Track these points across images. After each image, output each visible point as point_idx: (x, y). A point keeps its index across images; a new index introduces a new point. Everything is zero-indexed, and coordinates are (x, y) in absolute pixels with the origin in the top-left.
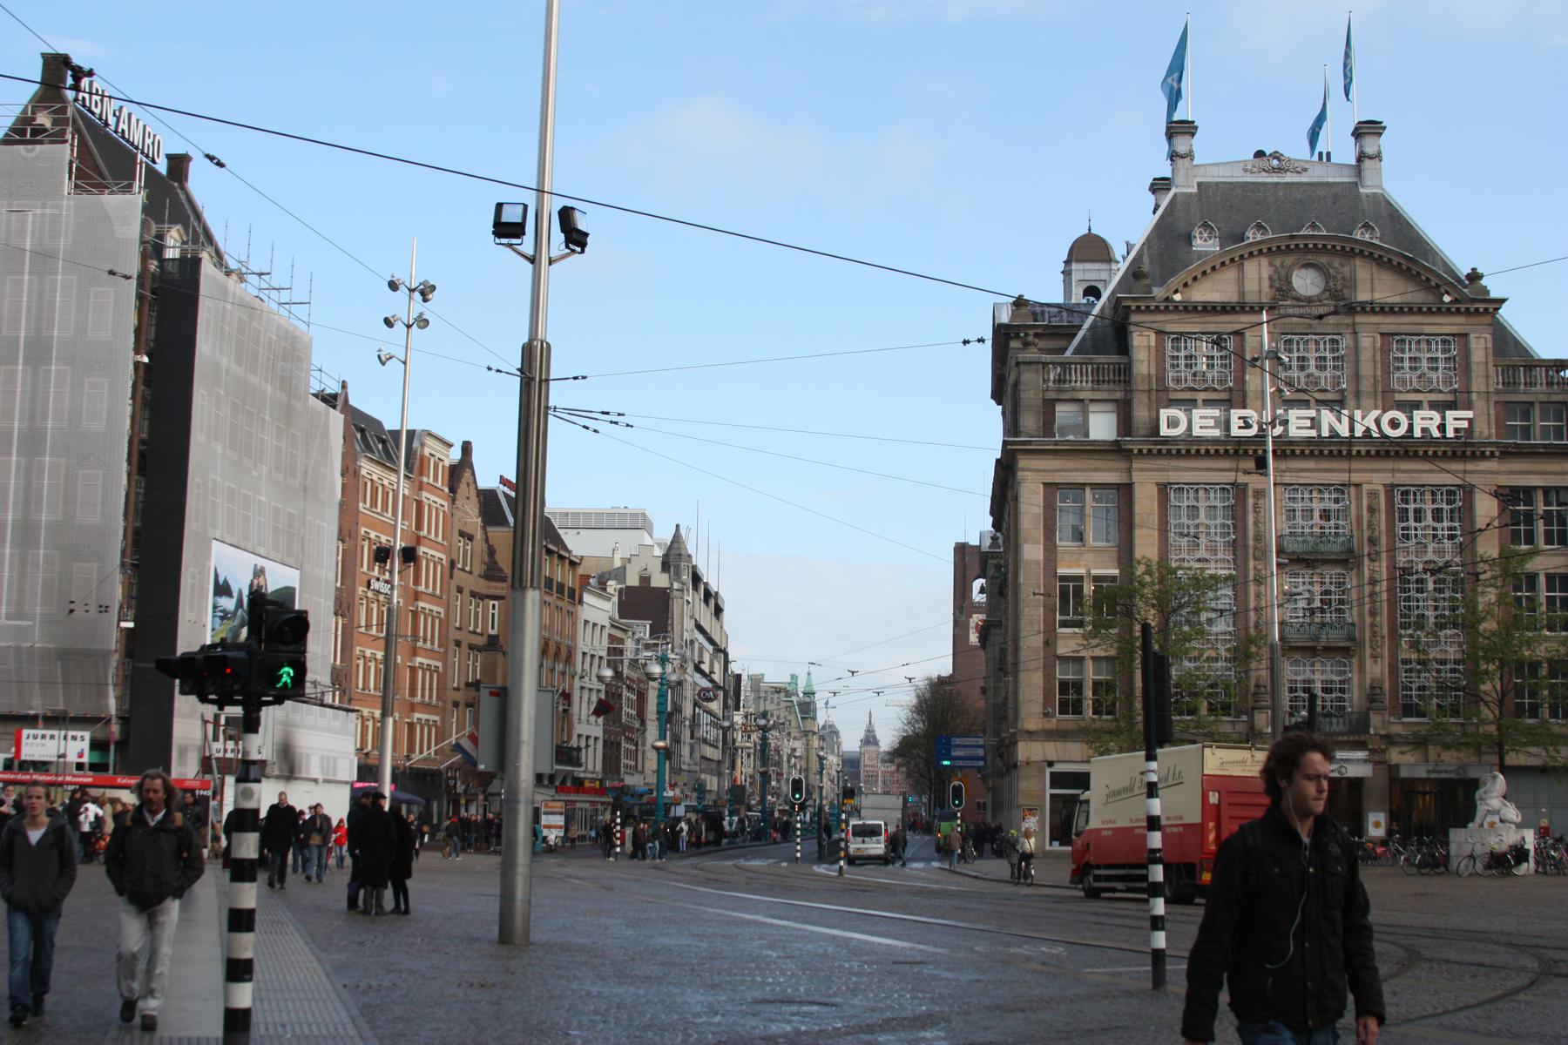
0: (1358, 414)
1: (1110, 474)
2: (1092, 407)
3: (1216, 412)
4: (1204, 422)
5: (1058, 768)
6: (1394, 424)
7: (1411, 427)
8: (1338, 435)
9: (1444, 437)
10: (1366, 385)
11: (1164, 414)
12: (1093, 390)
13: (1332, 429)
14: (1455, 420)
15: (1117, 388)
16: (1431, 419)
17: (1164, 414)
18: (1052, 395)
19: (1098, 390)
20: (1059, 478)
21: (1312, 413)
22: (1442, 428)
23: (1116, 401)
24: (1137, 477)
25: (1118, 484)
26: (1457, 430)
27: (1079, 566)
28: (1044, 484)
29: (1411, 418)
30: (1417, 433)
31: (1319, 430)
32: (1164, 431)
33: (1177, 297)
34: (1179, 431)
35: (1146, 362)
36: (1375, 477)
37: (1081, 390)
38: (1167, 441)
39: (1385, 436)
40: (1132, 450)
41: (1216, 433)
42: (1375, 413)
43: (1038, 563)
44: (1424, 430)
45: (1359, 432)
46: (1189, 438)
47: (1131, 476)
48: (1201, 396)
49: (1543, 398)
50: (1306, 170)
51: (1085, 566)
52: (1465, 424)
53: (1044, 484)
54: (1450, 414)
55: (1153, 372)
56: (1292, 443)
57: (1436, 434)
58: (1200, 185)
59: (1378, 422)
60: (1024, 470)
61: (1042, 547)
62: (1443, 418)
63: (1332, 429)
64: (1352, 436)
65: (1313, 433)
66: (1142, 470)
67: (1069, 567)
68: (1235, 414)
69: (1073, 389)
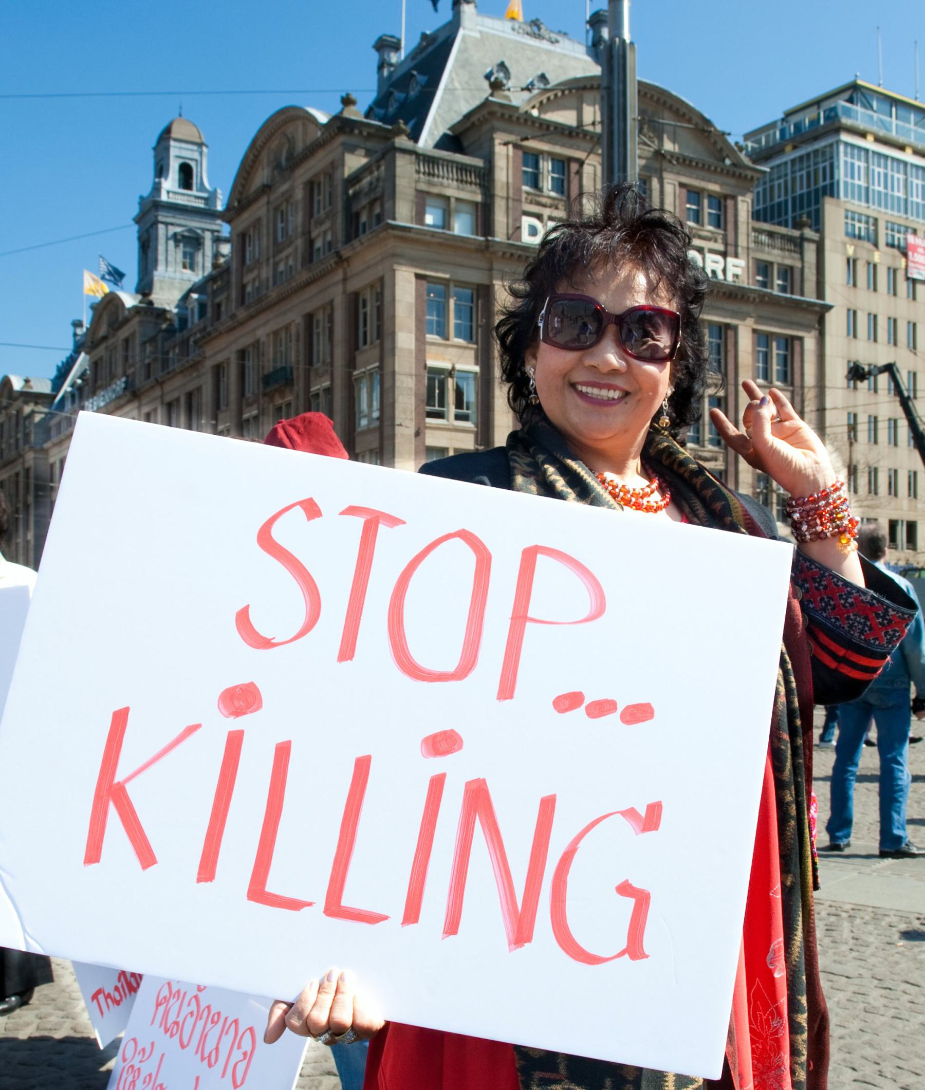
11: (526, 221)
12: (458, 188)
16: (716, 262)
17: (526, 221)
18: (423, 187)
19: (463, 190)
22: (724, 271)
27: (444, 359)
33: (535, 113)
35: (505, 171)
37: (448, 187)
43: (410, 351)
50: (557, 41)
51: (450, 360)
52: (739, 271)
54: (731, 260)
55: (511, 180)
57: (720, 276)
58: (481, 32)
61: (413, 336)
67: (436, 359)
69: (442, 185)
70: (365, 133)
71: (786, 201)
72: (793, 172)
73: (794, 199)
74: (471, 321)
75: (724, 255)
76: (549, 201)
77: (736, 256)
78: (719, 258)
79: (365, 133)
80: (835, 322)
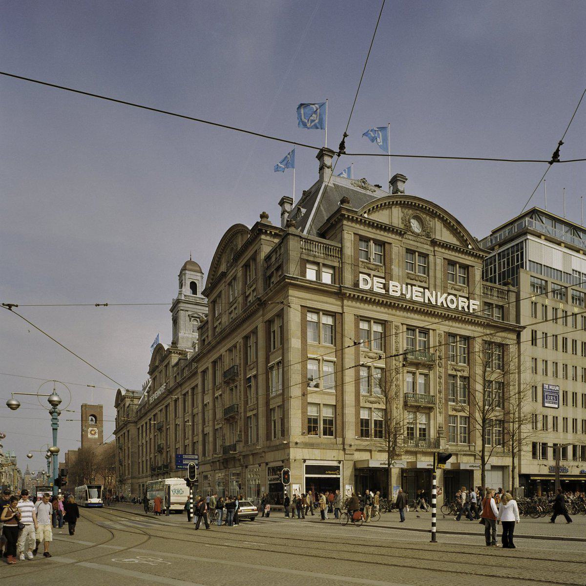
0: (439, 294)
1: (332, 305)
2: (324, 269)
3: (383, 281)
4: (377, 285)
5: (309, 463)
6: (452, 301)
7: (457, 306)
8: (431, 303)
9: (469, 312)
10: (438, 282)
11: (362, 276)
13: (429, 300)
14: (475, 305)
15: (335, 260)
17: (362, 276)
20: (309, 304)
21: (422, 290)
22: (468, 307)
23: (333, 268)
24: (346, 309)
25: (336, 313)
26: (474, 309)
28: (301, 306)
29: (458, 300)
30: (460, 309)
31: (424, 300)
32: (362, 286)
34: (367, 287)
36: (444, 327)
38: (362, 291)
39: (448, 307)
40: (346, 293)
41: (383, 291)
42: (445, 295)
44: (463, 308)
45: (439, 304)
46: (371, 291)
47: (343, 309)
48: (372, 273)
49: (496, 303)
52: (475, 307)
53: (301, 306)
56: (414, 302)
59: (446, 300)
60: (291, 296)
62: (469, 303)
63: (429, 300)
64: (436, 305)
65: (421, 300)
66: (349, 306)
68: (391, 283)
70: (273, 233)
71: (495, 276)
72: (499, 260)
73: (499, 274)
74: (332, 334)
75: (468, 299)
76: (374, 267)
77: (474, 299)
78: (465, 300)
79: (273, 233)
80: (526, 335)
